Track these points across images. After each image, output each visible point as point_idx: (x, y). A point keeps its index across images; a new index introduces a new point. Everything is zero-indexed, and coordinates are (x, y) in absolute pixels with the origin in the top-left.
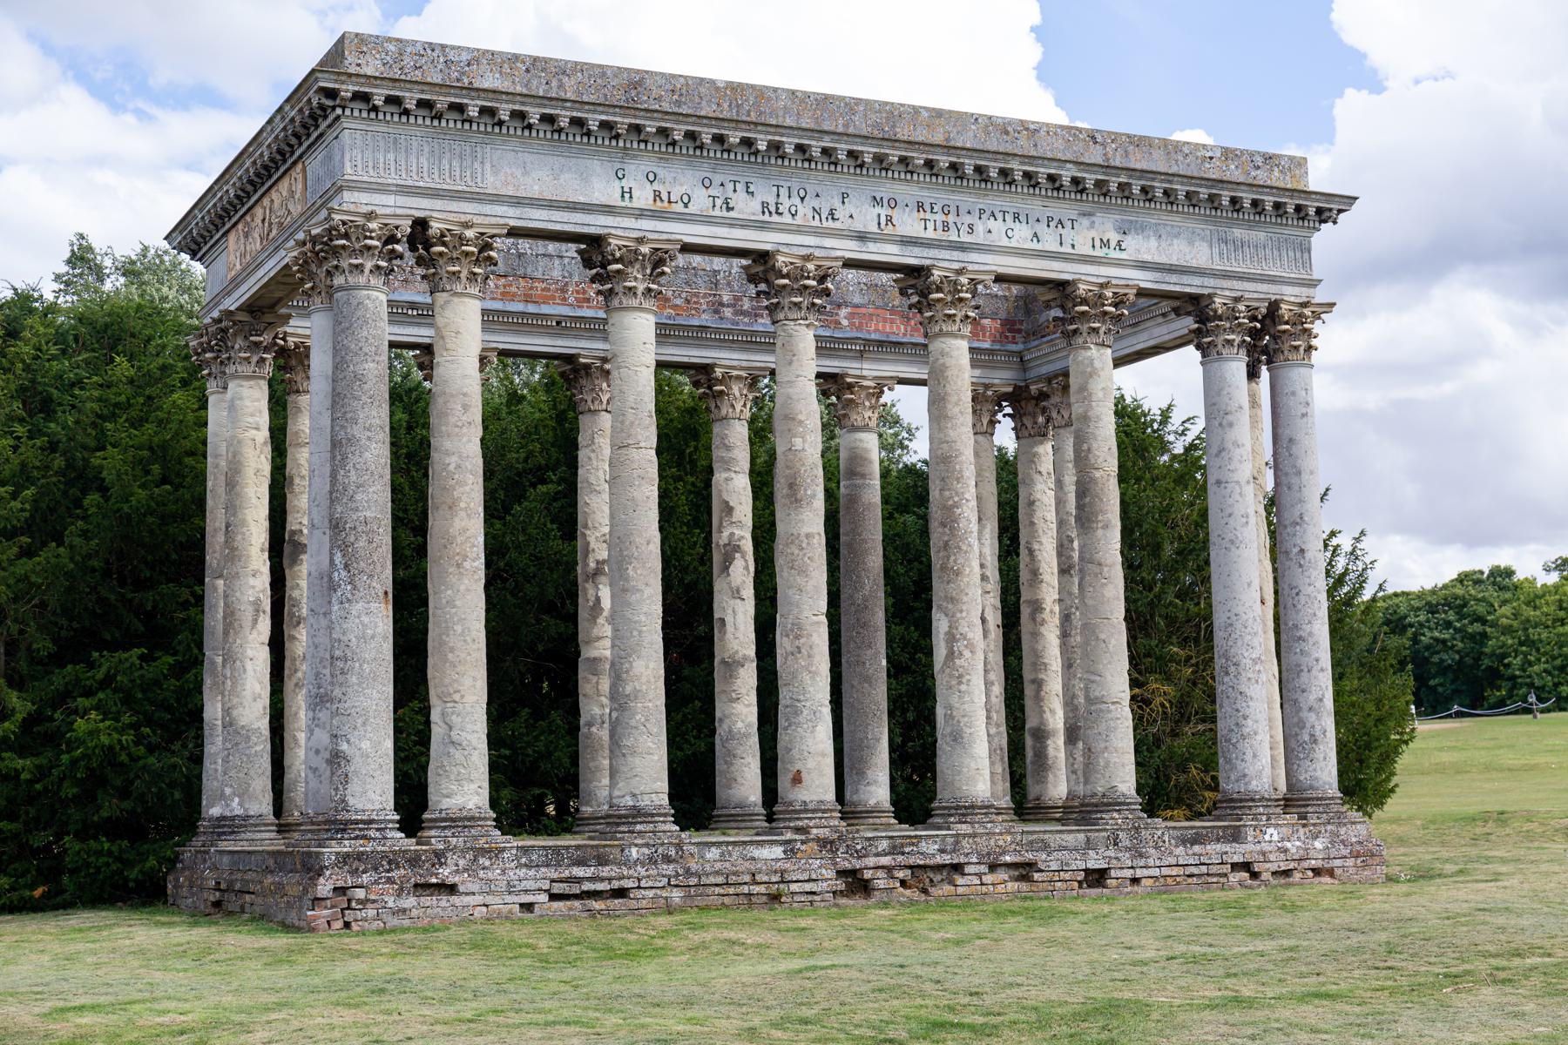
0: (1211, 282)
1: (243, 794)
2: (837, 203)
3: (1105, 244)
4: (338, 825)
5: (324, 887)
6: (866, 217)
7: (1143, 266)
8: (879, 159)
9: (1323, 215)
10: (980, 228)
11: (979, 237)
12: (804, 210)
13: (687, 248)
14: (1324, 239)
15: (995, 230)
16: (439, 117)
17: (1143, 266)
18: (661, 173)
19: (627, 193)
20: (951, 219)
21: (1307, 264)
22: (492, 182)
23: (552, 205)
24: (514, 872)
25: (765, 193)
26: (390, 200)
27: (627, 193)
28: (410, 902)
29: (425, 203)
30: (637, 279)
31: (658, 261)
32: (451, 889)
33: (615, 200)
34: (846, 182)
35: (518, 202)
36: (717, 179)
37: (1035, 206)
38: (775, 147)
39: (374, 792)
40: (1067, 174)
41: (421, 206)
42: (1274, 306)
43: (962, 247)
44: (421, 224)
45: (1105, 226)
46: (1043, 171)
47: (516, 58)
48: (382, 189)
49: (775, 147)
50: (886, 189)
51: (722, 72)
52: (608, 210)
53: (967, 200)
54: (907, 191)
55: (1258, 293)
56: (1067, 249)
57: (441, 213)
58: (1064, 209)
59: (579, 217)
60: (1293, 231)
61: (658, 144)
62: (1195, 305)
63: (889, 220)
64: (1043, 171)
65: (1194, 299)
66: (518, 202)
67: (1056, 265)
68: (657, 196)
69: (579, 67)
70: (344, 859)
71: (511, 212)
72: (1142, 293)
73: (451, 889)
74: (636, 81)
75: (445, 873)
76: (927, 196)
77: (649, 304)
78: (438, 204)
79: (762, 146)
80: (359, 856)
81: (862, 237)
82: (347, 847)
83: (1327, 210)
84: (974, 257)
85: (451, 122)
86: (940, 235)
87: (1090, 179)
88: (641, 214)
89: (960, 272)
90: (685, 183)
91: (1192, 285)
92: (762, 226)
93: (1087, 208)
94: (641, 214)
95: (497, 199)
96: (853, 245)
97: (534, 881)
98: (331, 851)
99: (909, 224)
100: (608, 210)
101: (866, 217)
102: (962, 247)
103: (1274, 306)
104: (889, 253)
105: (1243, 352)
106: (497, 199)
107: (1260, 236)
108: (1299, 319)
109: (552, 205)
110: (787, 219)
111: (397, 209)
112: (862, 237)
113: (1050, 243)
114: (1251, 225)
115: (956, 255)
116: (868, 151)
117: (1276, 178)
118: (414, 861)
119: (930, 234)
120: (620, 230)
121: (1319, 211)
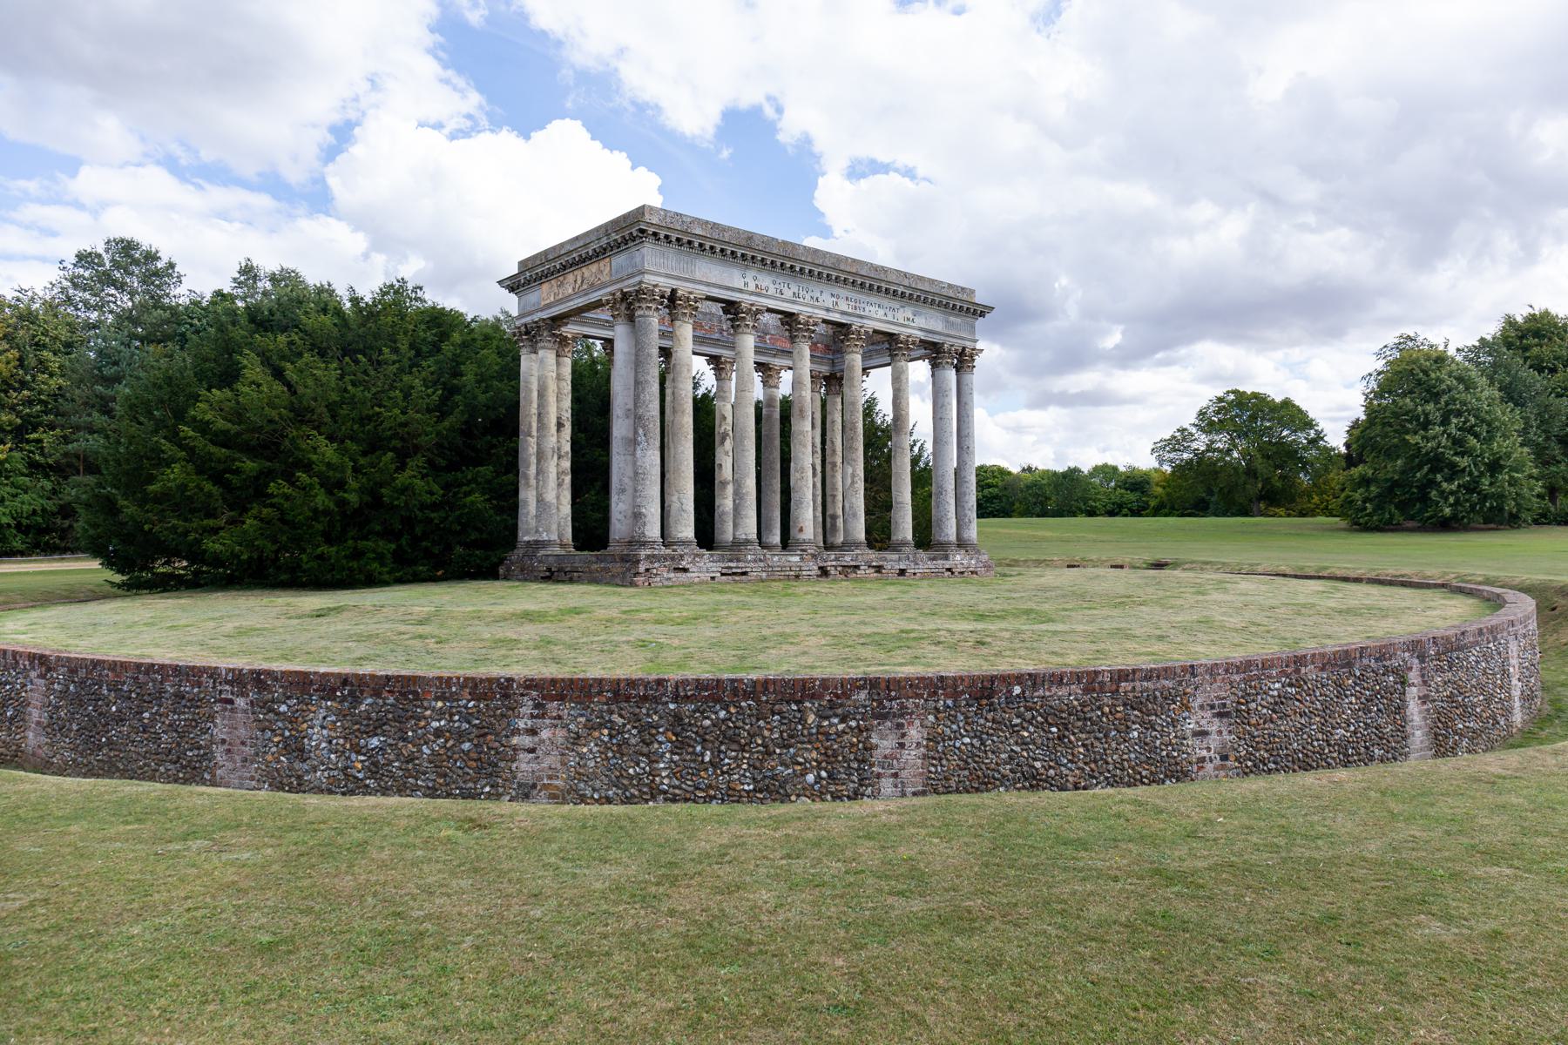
1: (548, 531)
4: (644, 544)
5: (642, 569)
6: (828, 301)
7: (921, 329)
9: (982, 314)
12: (808, 297)
15: (872, 311)
17: (921, 329)
19: (746, 284)
21: (974, 333)
22: (698, 276)
23: (720, 287)
24: (706, 565)
25: (794, 288)
27: (746, 284)
28: (672, 575)
32: (685, 570)
35: (708, 284)
37: (886, 302)
39: (653, 531)
41: (675, 283)
43: (861, 317)
44: (674, 291)
45: (908, 312)
47: (707, 222)
48: (659, 274)
50: (836, 291)
52: (740, 291)
53: (863, 297)
54: (843, 292)
55: (959, 344)
57: (683, 288)
58: (896, 305)
61: (758, 265)
65: (935, 344)
66: (708, 284)
69: (730, 229)
70: (648, 557)
73: (685, 570)
74: (750, 236)
75: (684, 564)
76: (850, 295)
80: (654, 556)
81: (828, 310)
82: (649, 552)
90: (766, 281)
91: (936, 338)
92: (794, 302)
94: (752, 293)
95: (700, 282)
97: (716, 567)
98: (643, 553)
99: (843, 306)
100: (740, 291)
101: (828, 301)
102: (861, 317)
106: (700, 282)
107: (958, 320)
108: (971, 356)
109: (720, 287)
111: (666, 284)
112: (828, 310)
114: (957, 316)
117: (965, 297)
118: (673, 559)
120: (746, 300)
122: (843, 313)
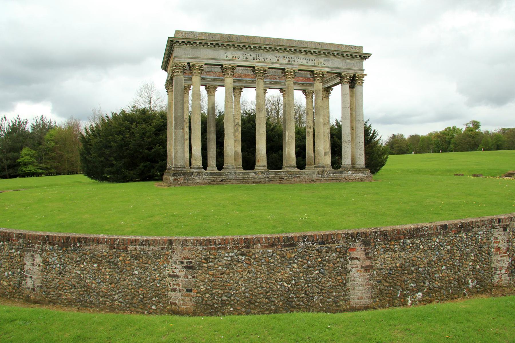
0: (342, 70)
2: (268, 57)
3: (321, 63)
7: (328, 67)
8: (275, 49)
10: (296, 61)
11: (296, 63)
13: (238, 66)
14: (366, 63)
16: (192, 44)
18: (234, 53)
20: (290, 59)
22: (201, 56)
23: (213, 59)
25: (254, 55)
26: (183, 60)
29: (190, 60)
30: (229, 72)
31: (233, 69)
33: (225, 57)
34: (270, 53)
35: (207, 59)
36: (245, 53)
38: (255, 47)
40: (312, 51)
41: (189, 61)
42: (354, 75)
45: (321, 60)
46: (308, 50)
48: (182, 58)
49: (255, 47)
51: (245, 34)
52: (224, 60)
54: (282, 55)
56: (313, 65)
57: (192, 62)
58: (313, 57)
59: (218, 61)
60: (359, 60)
62: (339, 75)
63: (278, 60)
64: (308, 50)
66: (207, 59)
67: (311, 68)
68: (233, 57)
71: (206, 61)
72: (328, 72)
76: (285, 55)
77: (231, 76)
78: (192, 60)
79: (252, 47)
81: (272, 63)
83: (366, 56)
84: (295, 66)
85: (194, 45)
86: (288, 62)
87: (317, 51)
88: (230, 60)
89: (291, 69)
90: (238, 54)
91: (339, 71)
93: (317, 57)
94: (230, 60)
95: (203, 58)
96: (271, 64)
99: (282, 61)
102: (292, 65)
103: (354, 75)
104: (278, 66)
105: (348, 83)
106: (203, 58)
109: (213, 59)
110: (258, 60)
111: (185, 61)
112: (272, 63)
113: (310, 64)
114: (351, 59)
115: (291, 66)
116: (273, 47)
119: (286, 62)
120: (225, 63)
121: (364, 57)
122: (281, 64)
